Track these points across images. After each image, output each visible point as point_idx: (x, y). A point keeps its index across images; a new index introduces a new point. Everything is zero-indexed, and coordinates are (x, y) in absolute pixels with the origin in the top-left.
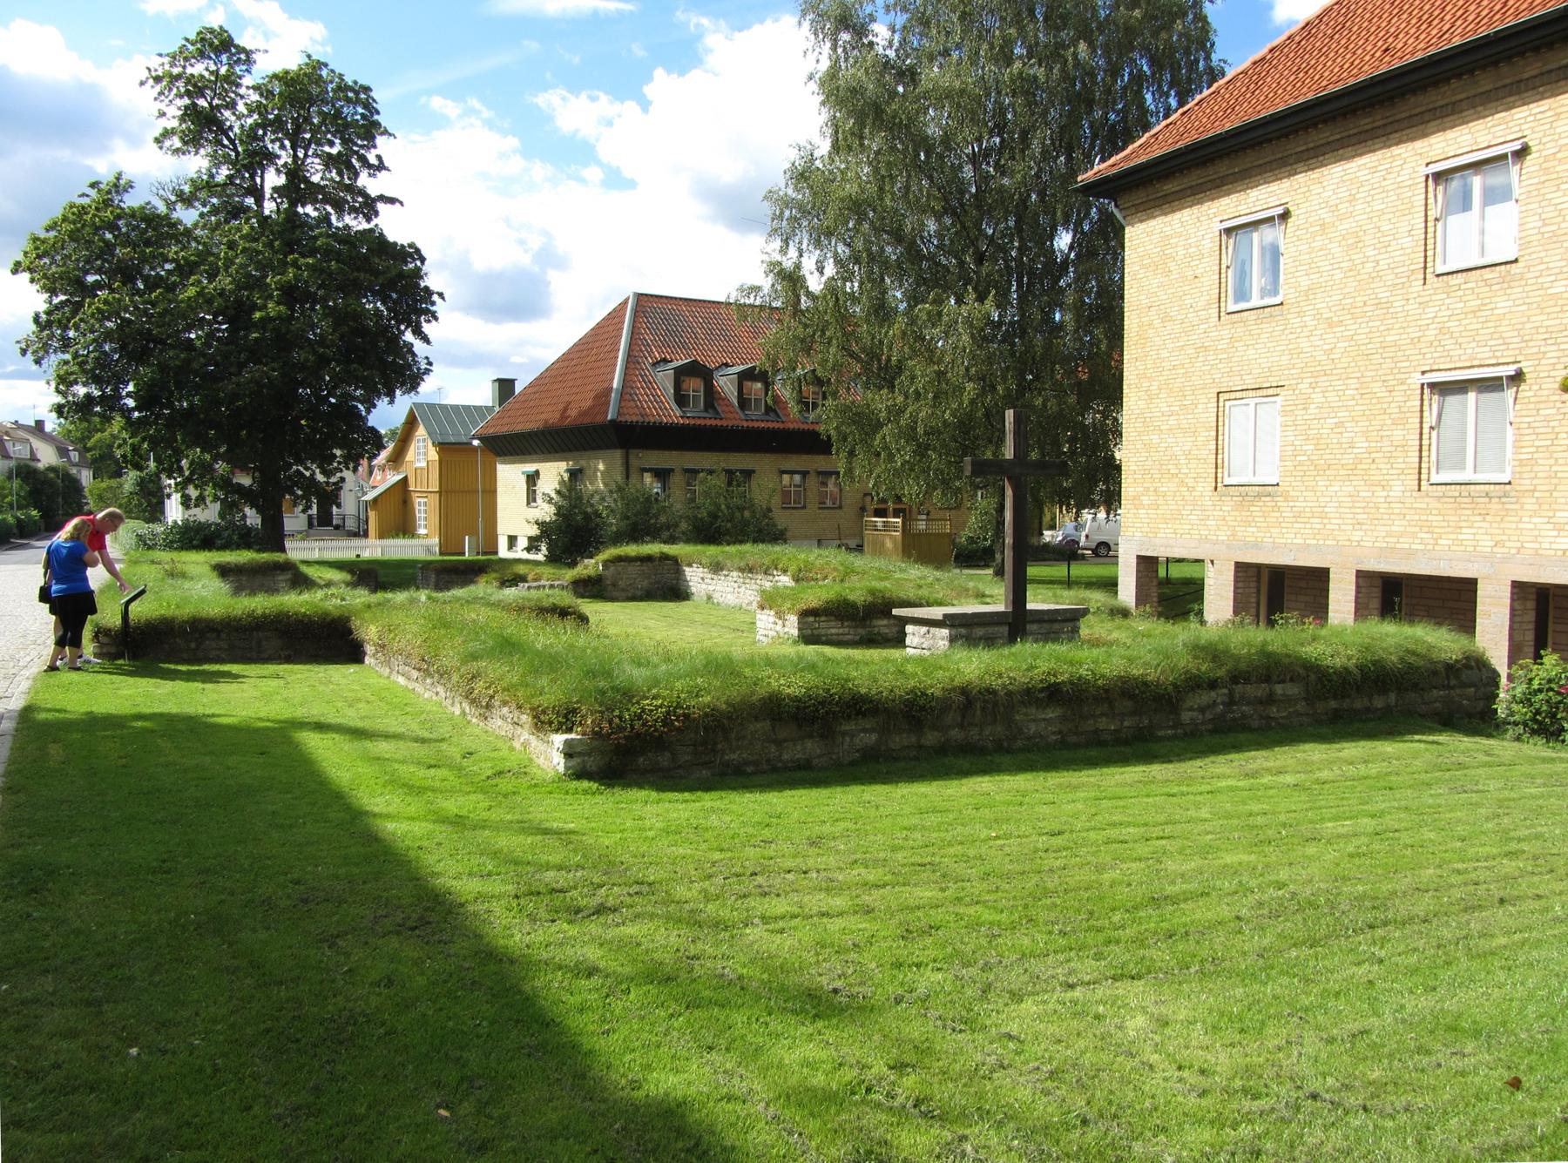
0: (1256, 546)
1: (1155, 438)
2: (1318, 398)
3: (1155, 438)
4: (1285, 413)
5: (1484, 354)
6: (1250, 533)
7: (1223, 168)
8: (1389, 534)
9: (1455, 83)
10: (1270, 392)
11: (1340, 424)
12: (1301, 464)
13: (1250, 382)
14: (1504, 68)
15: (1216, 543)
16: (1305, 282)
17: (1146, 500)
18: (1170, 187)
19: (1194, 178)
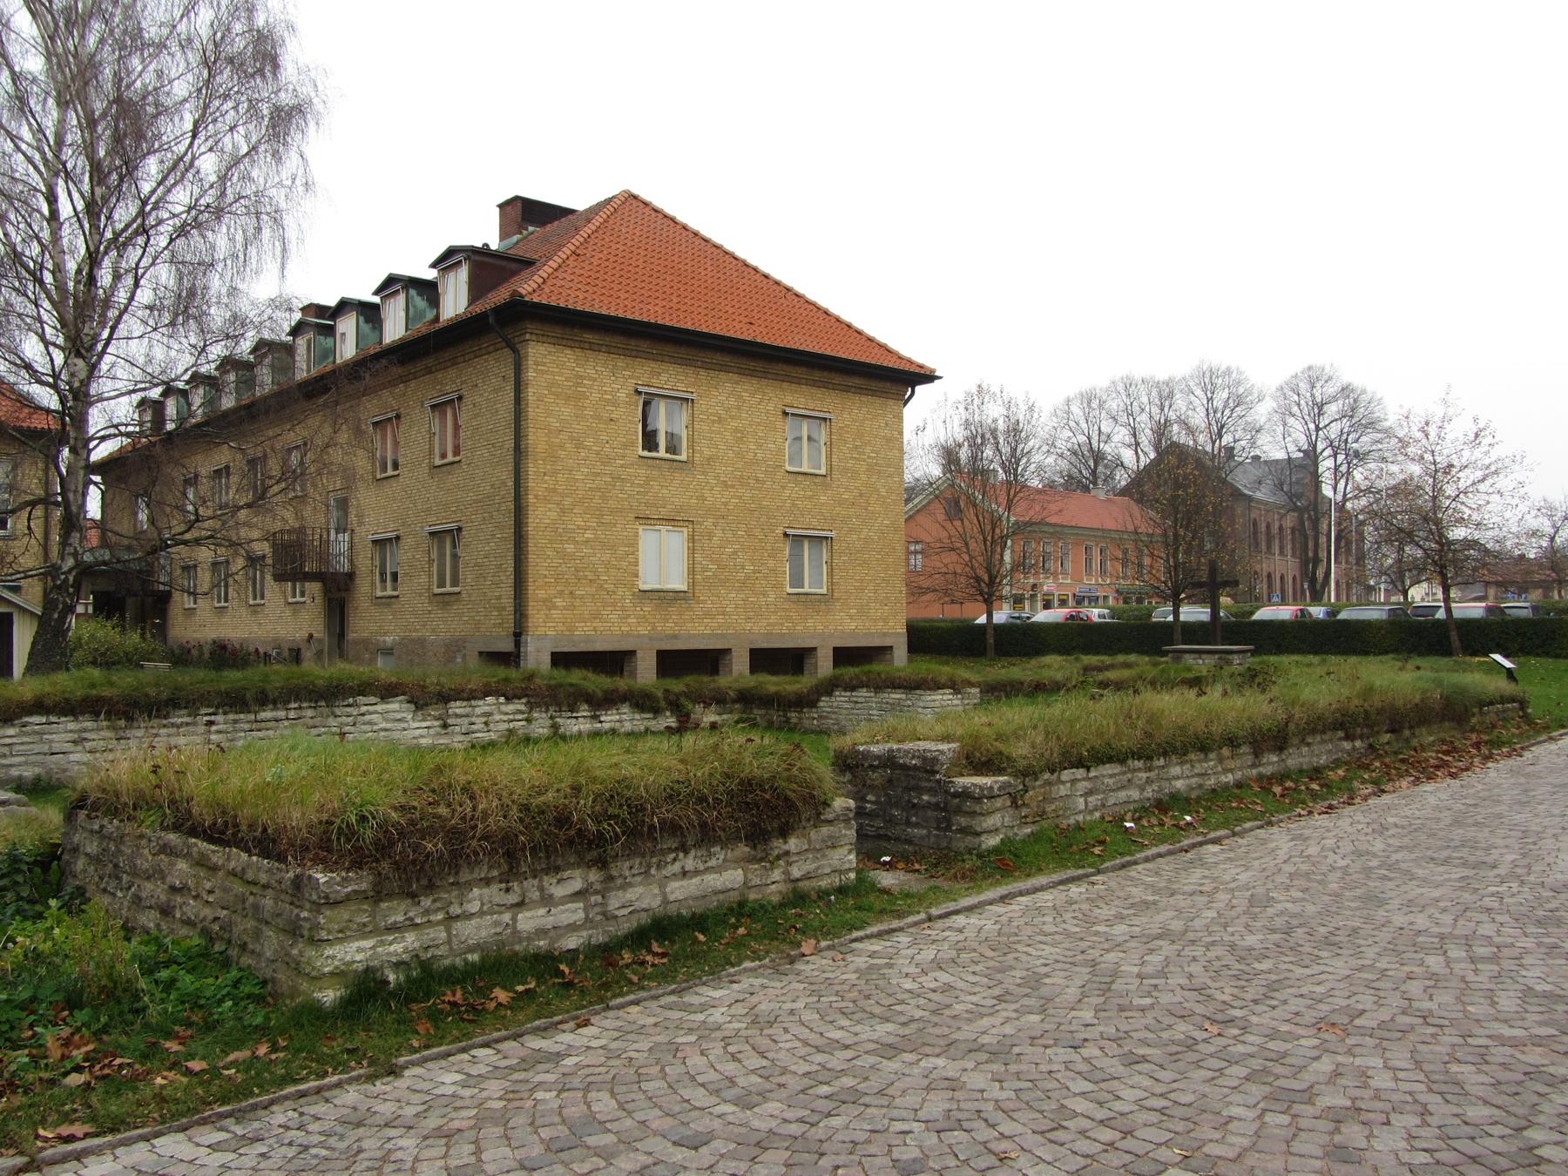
0: (675, 637)
1: (570, 548)
2: (719, 533)
3: (570, 548)
4: (692, 539)
5: (815, 523)
6: (669, 627)
7: (644, 345)
8: (768, 625)
9: (804, 369)
10: (681, 523)
11: (735, 553)
12: (708, 577)
13: (664, 513)
14: (826, 374)
15: (639, 636)
16: (707, 452)
17: (559, 602)
18: (588, 336)
19: (616, 340)
